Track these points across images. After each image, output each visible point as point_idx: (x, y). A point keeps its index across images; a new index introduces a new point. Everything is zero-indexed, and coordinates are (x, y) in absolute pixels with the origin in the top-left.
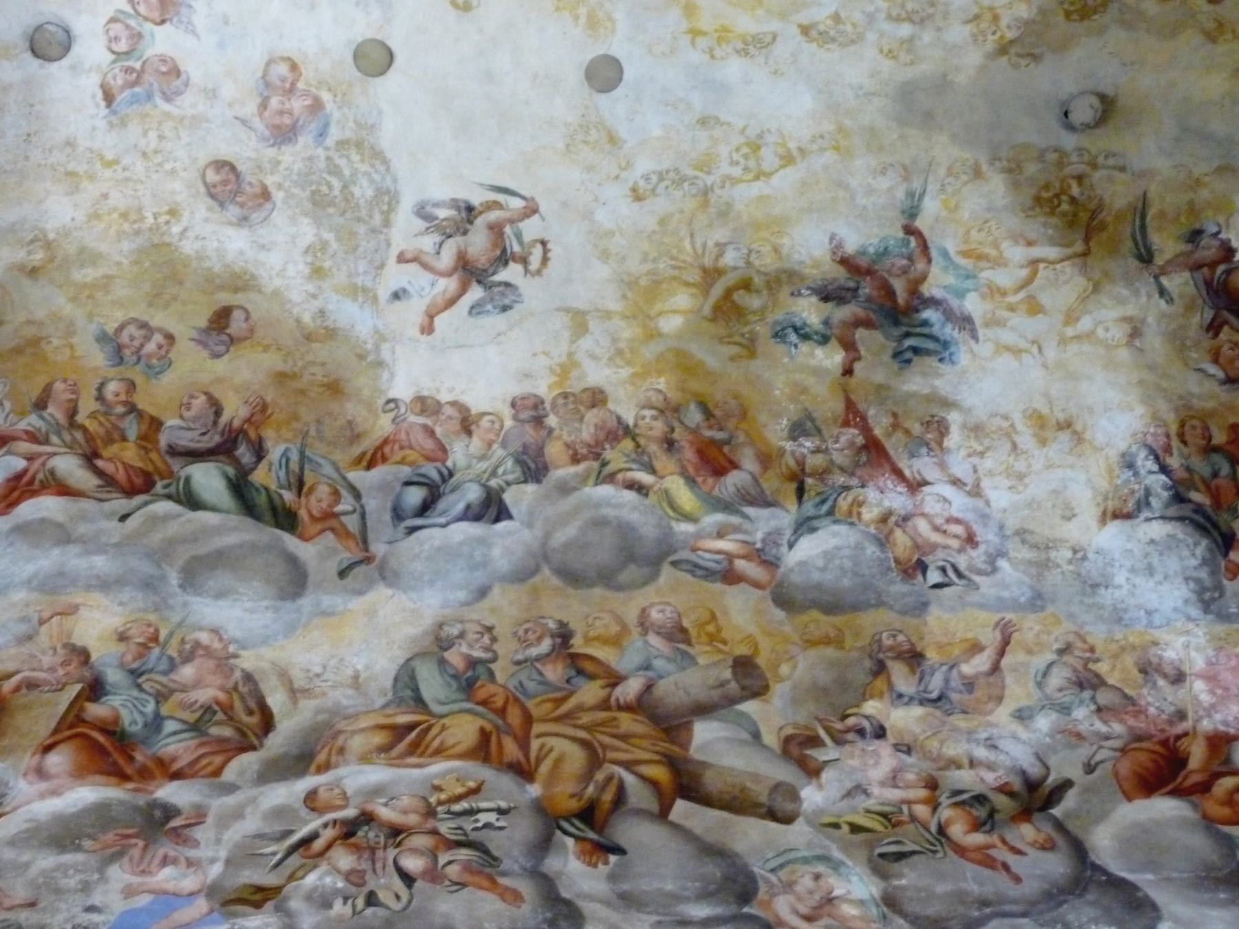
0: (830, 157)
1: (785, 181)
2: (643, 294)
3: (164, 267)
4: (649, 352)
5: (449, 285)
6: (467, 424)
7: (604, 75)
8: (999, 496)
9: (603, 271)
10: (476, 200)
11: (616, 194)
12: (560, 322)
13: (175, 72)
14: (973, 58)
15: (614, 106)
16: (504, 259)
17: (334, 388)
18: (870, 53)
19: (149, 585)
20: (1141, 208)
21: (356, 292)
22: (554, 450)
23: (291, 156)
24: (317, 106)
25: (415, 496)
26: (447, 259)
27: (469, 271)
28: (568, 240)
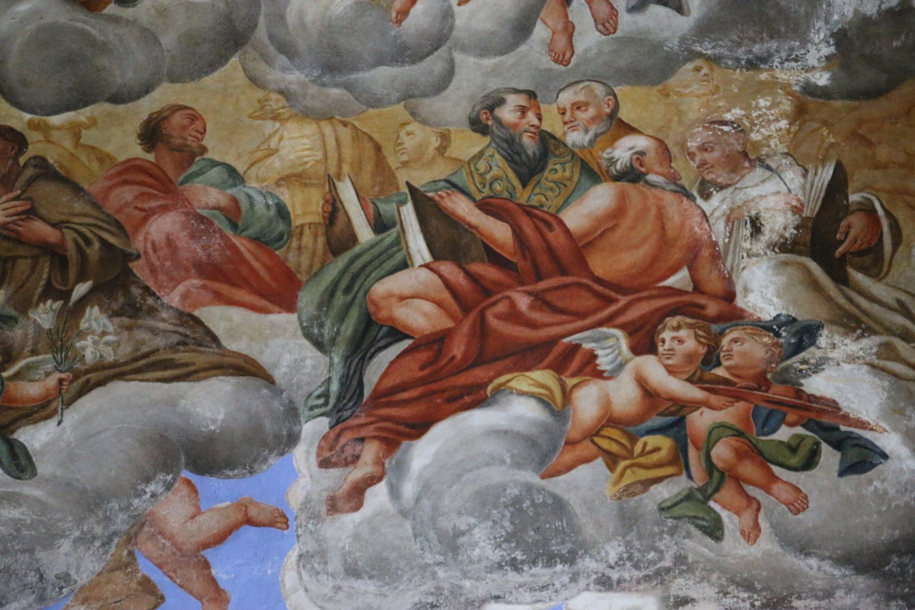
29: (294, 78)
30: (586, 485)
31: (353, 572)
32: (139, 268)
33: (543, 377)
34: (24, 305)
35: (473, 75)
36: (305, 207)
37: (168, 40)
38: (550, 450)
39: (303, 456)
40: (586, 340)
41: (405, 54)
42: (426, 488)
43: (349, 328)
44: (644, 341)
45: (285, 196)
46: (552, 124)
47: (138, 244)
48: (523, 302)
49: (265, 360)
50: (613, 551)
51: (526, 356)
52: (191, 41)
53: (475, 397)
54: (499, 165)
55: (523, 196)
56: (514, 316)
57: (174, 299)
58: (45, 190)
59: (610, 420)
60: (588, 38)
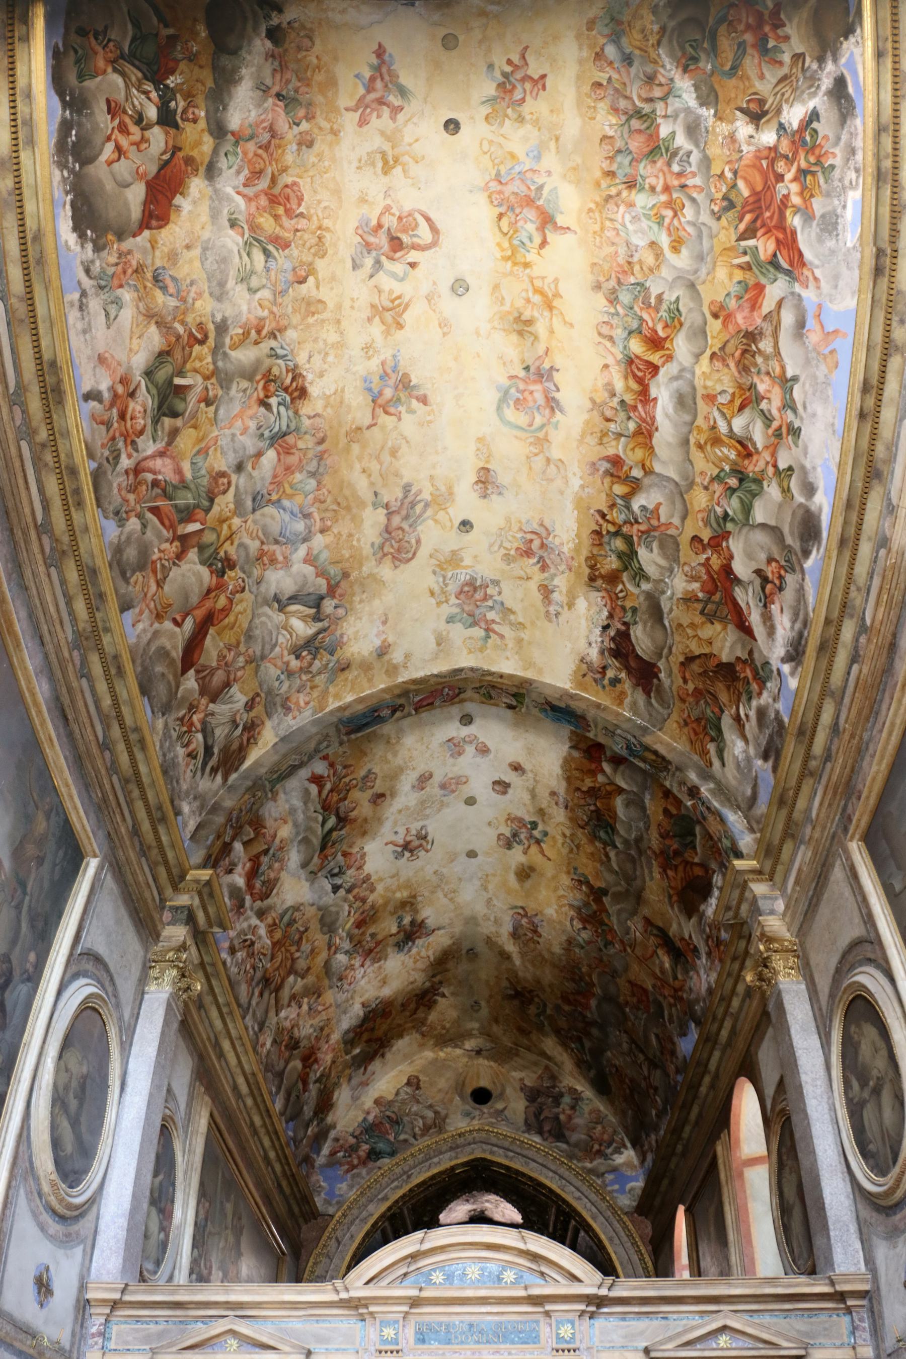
0: (452, 907)
1: (445, 901)
2: (407, 885)
3: (394, 776)
4: (389, 894)
5: (401, 842)
6: (360, 868)
7: (472, 854)
8: (363, 983)
9: (411, 874)
10: (429, 838)
11: (436, 867)
12: (394, 871)
13: (460, 754)
14: (486, 931)
15: (463, 858)
16: (411, 851)
17: (364, 833)
18: (485, 911)
19: (298, 834)
20: (447, 970)
21: (395, 823)
22: (356, 891)
23: (437, 791)
24: (453, 791)
25: (336, 871)
26: (408, 839)
27: (406, 846)
28: (418, 863)
29: (704, 271)
30: (818, 205)
31: (836, 287)
32: (750, 329)
33: (788, 212)
34: (756, 365)
35: (705, 217)
36: (739, 275)
37: (692, 305)
38: (808, 216)
39: (805, 293)
40: (779, 197)
41: (700, 236)
42: (817, 256)
43: (772, 270)
44: (780, 178)
45: (735, 280)
46: (719, 196)
47: (743, 327)
48: (768, 214)
49: (778, 298)
50: (836, 202)
51: (782, 217)
52: (692, 299)
53: (794, 233)
54: (730, 214)
55: (739, 208)
56: (771, 218)
57: (759, 321)
58: (727, 350)
59: (801, 194)
60: (697, 181)
